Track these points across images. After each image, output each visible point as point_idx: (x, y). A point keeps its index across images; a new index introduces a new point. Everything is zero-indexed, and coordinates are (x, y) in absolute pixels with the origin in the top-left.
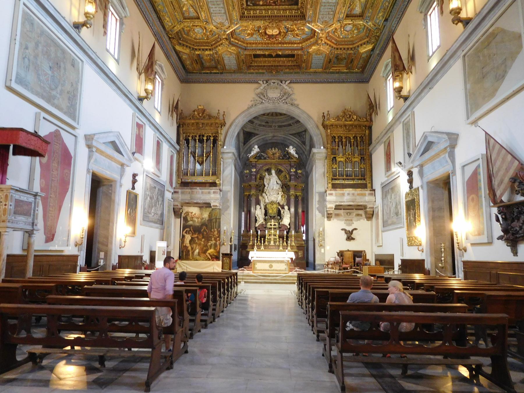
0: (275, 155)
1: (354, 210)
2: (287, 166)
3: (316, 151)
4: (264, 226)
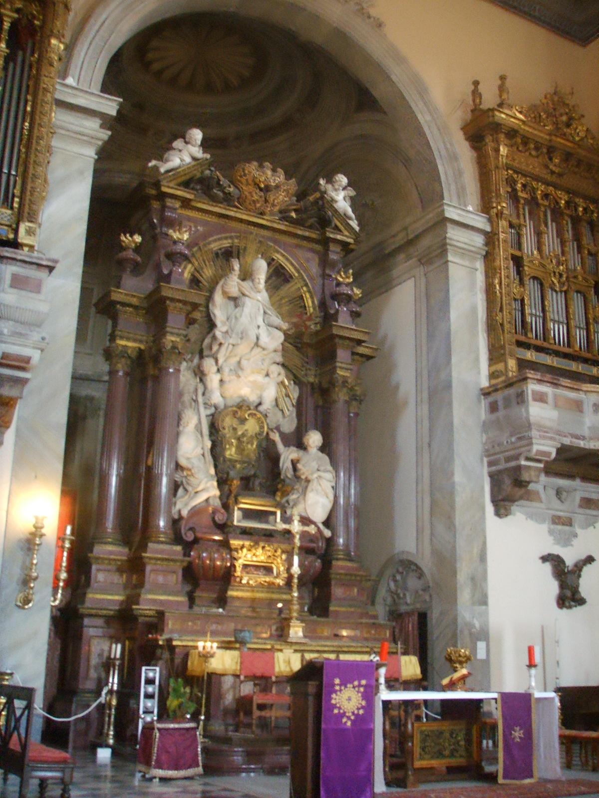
0: (271, 197)
1: (577, 483)
2: (308, 260)
3: (456, 218)
4: (220, 518)
